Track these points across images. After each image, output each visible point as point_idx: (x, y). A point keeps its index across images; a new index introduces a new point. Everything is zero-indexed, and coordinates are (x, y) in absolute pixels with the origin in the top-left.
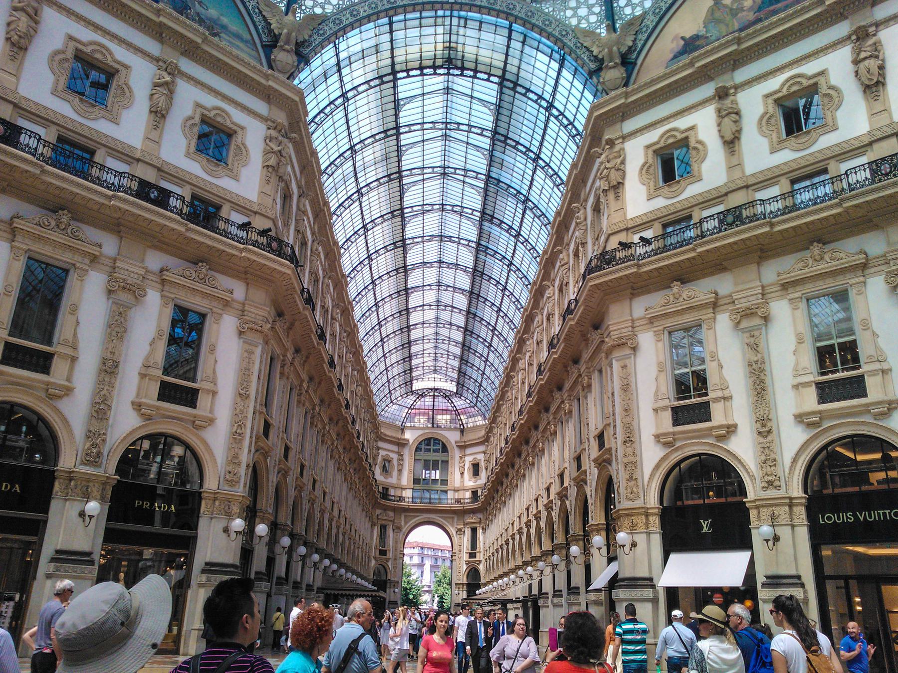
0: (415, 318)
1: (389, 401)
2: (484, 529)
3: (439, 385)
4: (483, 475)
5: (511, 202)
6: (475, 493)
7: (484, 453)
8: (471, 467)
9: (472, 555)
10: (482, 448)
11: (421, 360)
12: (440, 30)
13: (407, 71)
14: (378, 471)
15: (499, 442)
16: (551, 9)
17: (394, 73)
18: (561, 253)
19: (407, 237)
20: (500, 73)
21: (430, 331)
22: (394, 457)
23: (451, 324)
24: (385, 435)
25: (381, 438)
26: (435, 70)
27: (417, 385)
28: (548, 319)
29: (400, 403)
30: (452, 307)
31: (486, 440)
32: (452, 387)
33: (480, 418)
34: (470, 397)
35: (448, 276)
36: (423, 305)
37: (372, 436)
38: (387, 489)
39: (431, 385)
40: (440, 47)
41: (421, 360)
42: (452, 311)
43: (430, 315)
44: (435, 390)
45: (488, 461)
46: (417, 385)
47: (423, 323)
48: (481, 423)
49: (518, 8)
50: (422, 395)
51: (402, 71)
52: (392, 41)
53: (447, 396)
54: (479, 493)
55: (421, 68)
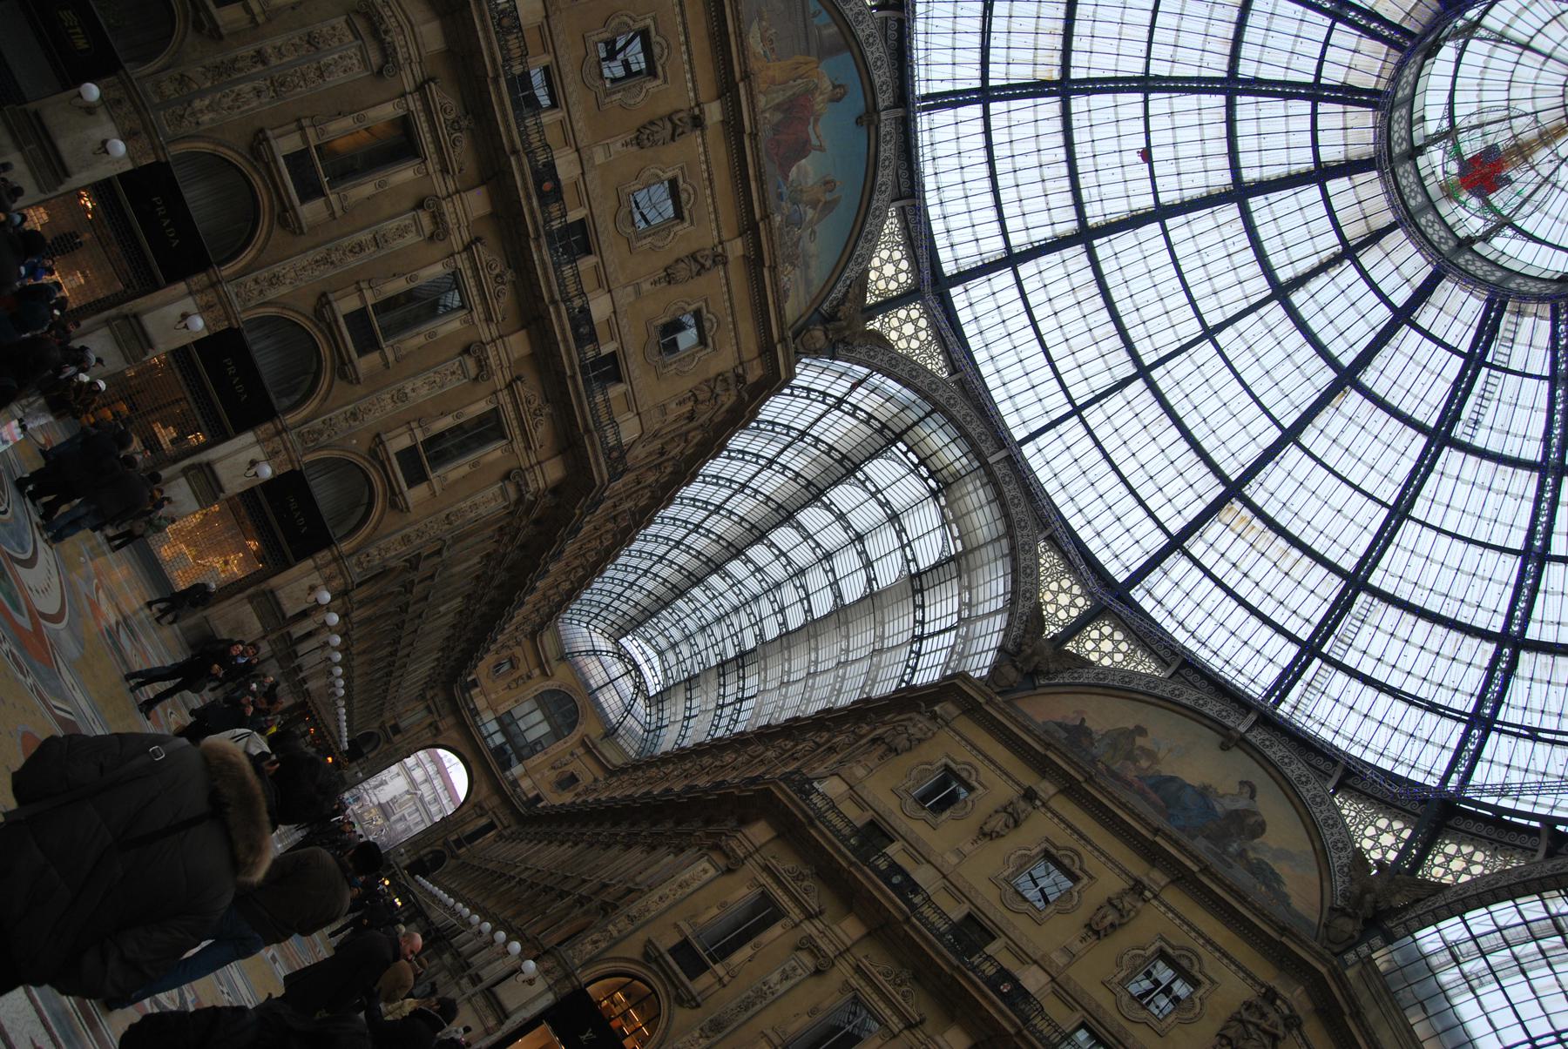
0: (759, 553)
1: (587, 619)
2: (500, 836)
3: (645, 668)
4: (567, 798)
5: (870, 636)
6: (538, 798)
7: (596, 780)
8: (568, 774)
9: (459, 843)
10: (600, 775)
11: (705, 600)
12: (964, 461)
13: (910, 449)
14: (489, 659)
15: (620, 790)
16: (1047, 565)
17: (899, 437)
18: (828, 731)
19: (865, 469)
20: (969, 547)
21: (753, 586)
22: (523, 669)
23: (782, 610)
24: (541, 642)
25: (534, 635)
26: (930, 477)
27: (630, 644)
28: (830, 748)
29: (593, 634)
30: (808, 596)
31: (613, 772)
32: (653, 685)
33: (636, 747)
34: (654, 718)
35: (847, 562)
36: (784, 554)
37: (528, 628)
38: (476, 686)
39: (640, 659)
40: (951, 469)
41: (705, 600)
42: (801, 600)
43: (777, 571)
44: (637, 667)
45: (587, 791)
46: (630, 644)
47: (759, 569)
48: (632, 753)
49: (1025, 532)
50: (622, 655)
51: (906, 444)
52: (921, 419)
53: (640, 687)
54: (539, 806)
55: (922, 462)
